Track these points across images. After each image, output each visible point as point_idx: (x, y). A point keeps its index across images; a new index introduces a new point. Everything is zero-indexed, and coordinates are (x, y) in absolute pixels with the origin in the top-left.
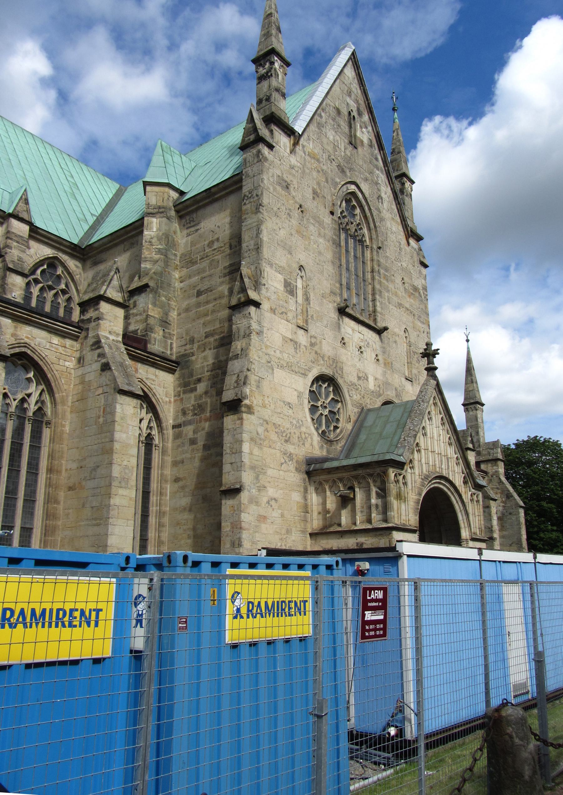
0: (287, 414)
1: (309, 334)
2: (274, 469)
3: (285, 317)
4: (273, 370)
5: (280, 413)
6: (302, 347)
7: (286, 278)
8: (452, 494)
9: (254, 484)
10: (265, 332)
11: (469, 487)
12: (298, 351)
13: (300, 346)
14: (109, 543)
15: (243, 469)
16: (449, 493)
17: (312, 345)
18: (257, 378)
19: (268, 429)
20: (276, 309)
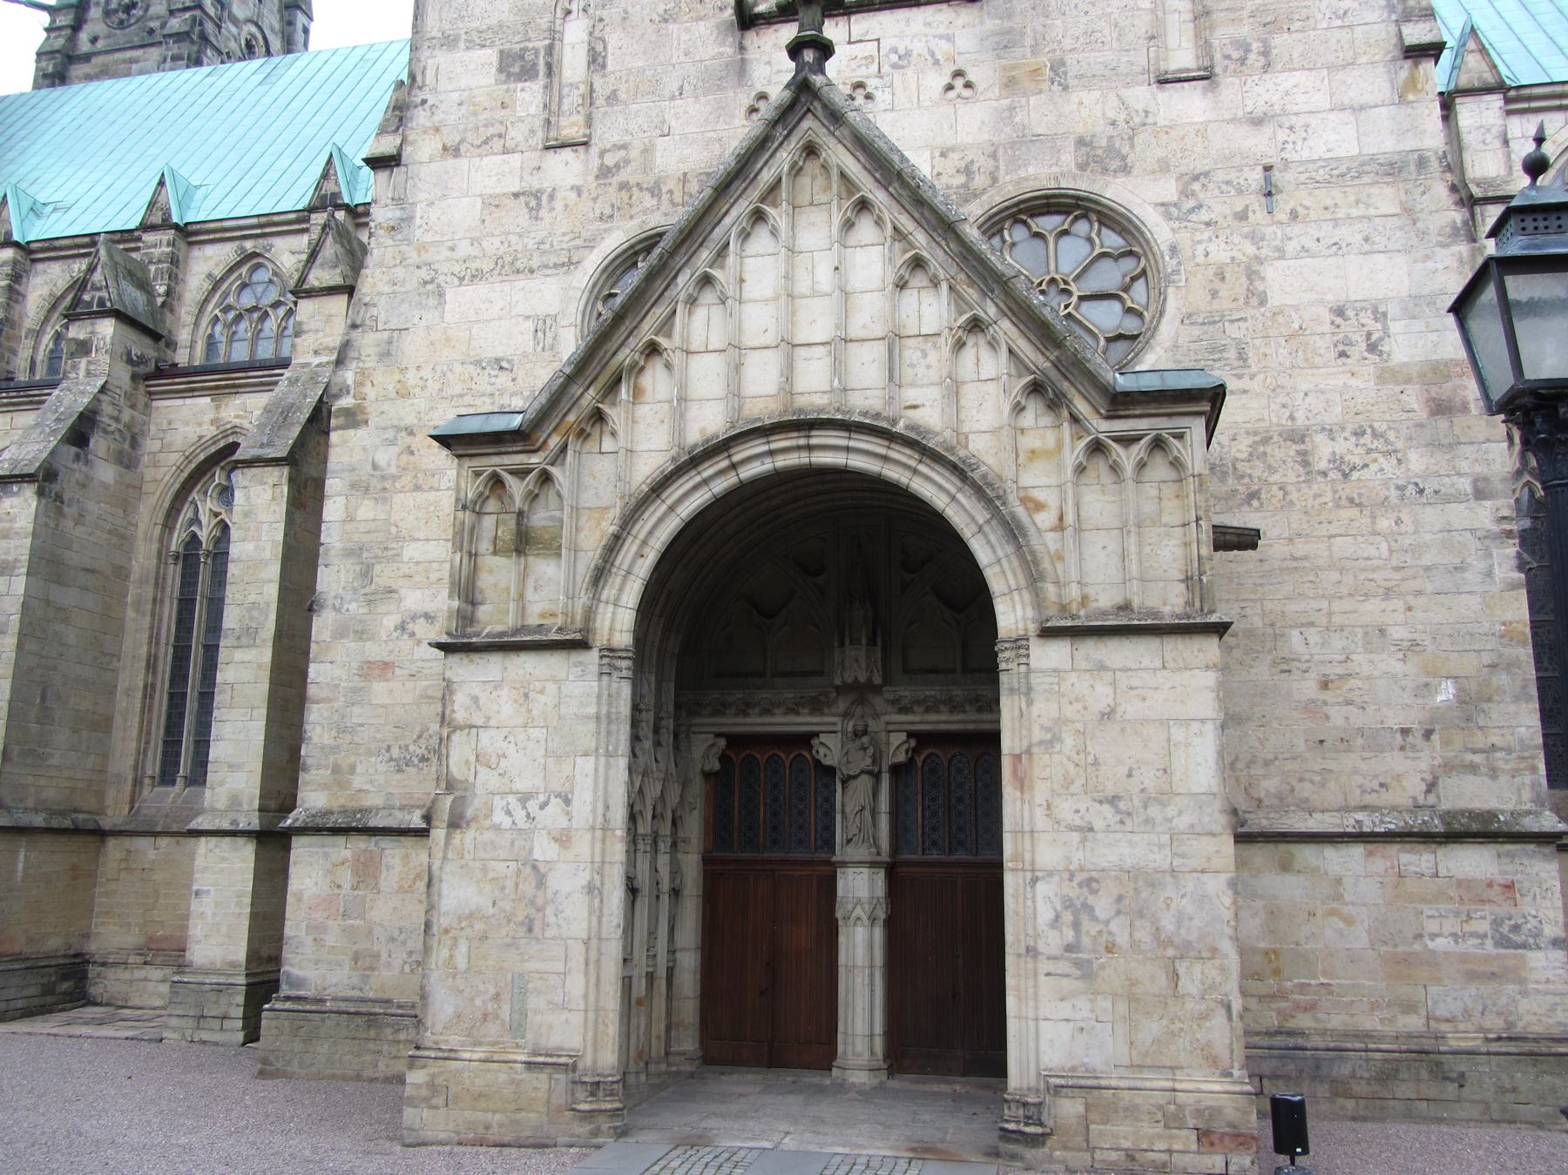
0: (489, 389)
1: (594, 150)
2: (428, 540)
3: (497, 145)
4: (441, 295)
5: (462, 396)
6: (559, 195)
7: (507, 46)
8: (915, 471)
9: (355, 590)
10: (418, 213)
11: (1075, 419)
12: (543, 213)
13: (552, 197)
14: (211, 757)
15: (320, 561)
16: (893, 473)
17: (605, 172)
18: (386, 335)
19: (413, 448)
20: (462, 141)
